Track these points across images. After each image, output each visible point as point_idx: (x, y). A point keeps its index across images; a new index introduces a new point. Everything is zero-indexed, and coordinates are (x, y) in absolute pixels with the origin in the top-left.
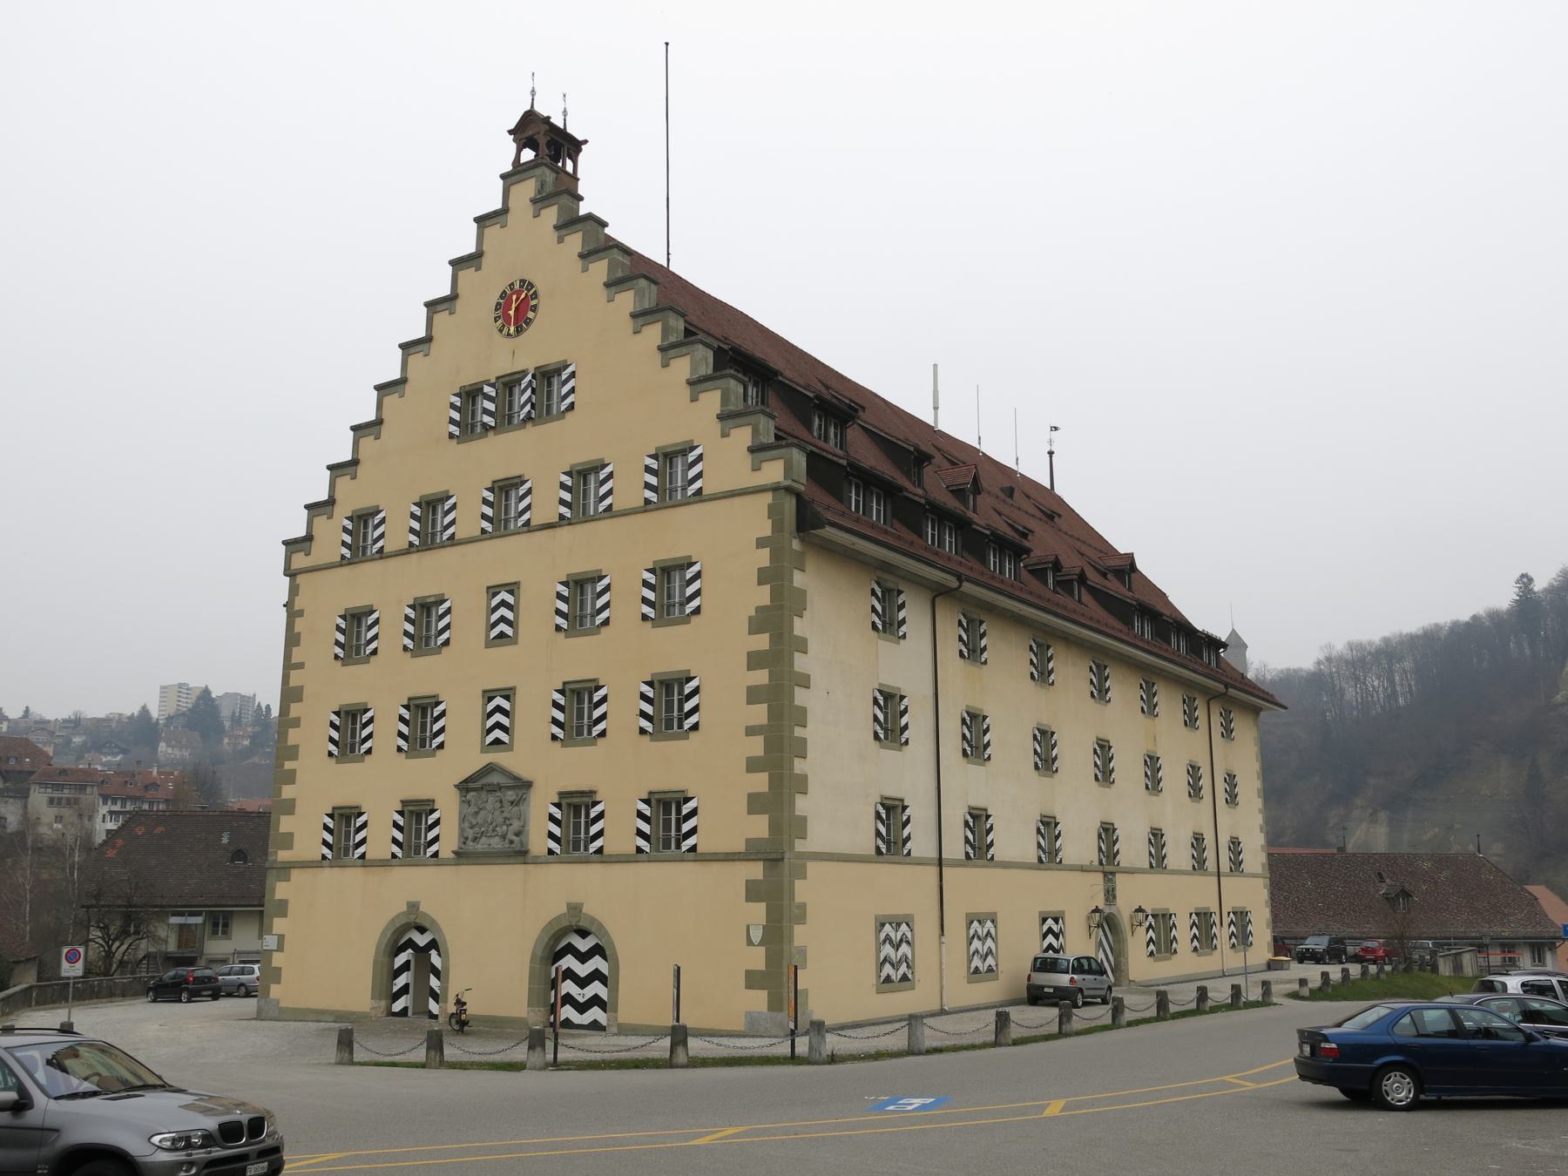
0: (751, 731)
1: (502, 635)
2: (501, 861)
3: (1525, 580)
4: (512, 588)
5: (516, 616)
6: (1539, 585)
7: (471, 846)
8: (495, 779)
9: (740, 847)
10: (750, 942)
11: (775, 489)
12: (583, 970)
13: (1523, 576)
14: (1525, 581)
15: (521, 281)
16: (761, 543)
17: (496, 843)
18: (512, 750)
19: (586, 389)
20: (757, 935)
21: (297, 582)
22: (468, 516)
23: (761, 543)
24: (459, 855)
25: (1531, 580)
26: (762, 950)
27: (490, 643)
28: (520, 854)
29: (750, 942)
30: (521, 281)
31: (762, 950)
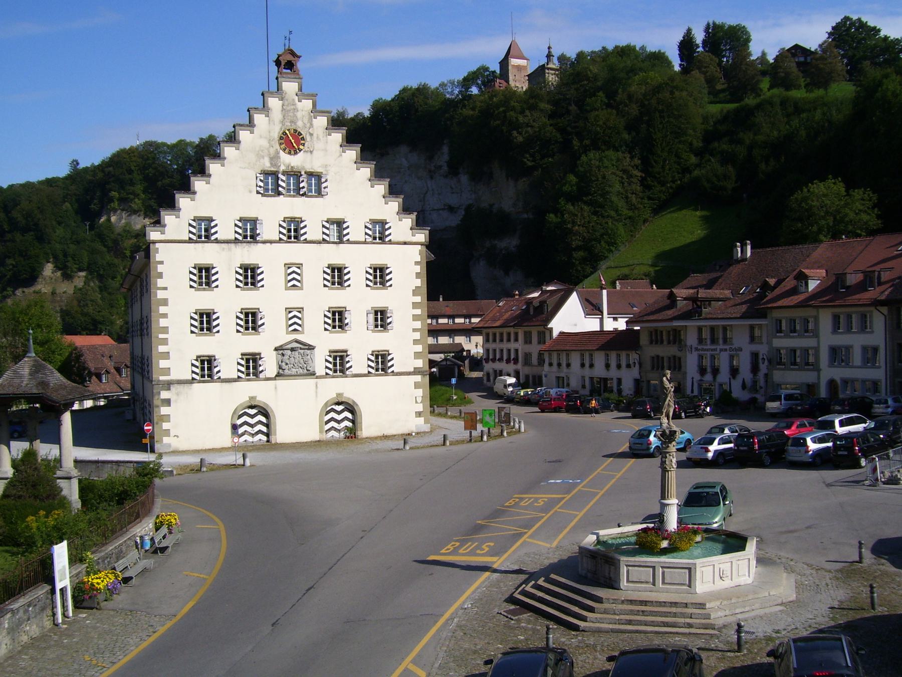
0: (414, 330)
1: (294, 286)
2: (308, 377)
3: (75, 163)
4: (299, 266)
5: (302, 278)
6: (82, 166)
7: (287, 372)
8: (295, 345)
9: (412, 370)
10: (416, 402)
11: (421, 244)
12: (339, 417)
13: (74, 161)
14: (75, 163)
15: (294, 130)
16: (417, 263)
17: (301, 371)
18: (304, 333)
19: (331, 186)
20: (419, 400)
21: (157, 247)
22: (269, 229)
23: (417, 263)
24: (278, 375)
25: (78, 164)
26: (422, 404)
27: (287, 289)
28: (312, 374)
29: (416, 402)
30: (294, 130)
31: (422, 404)
